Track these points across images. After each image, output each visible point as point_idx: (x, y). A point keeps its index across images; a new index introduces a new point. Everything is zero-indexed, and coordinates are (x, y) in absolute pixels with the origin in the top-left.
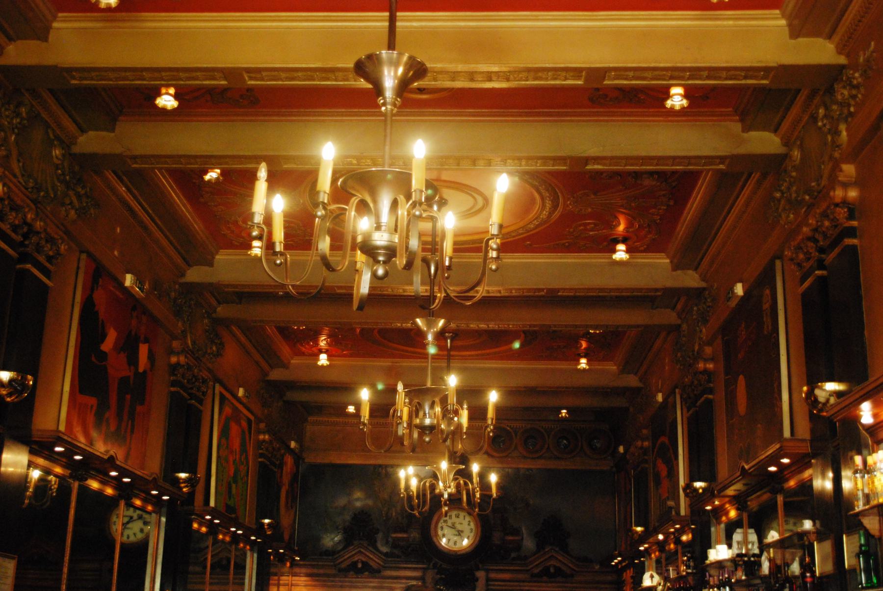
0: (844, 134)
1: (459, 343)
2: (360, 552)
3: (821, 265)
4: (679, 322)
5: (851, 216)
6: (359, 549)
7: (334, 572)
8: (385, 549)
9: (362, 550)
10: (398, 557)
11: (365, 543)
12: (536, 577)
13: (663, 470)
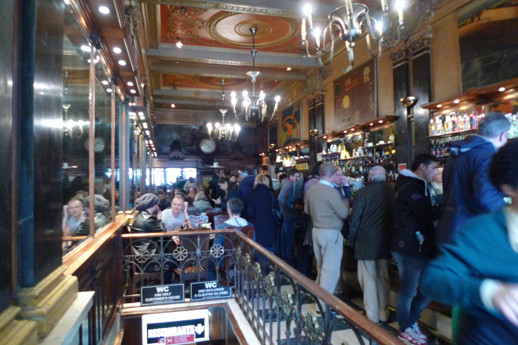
0: (433, 15)
1: (226, 84)
2: (177, 153)
3: (406, 59)
4: (306, 79)
5: (429, 43)
6: (176, 152)
7: (168, 160)
8: (184, 152)
9: (177, 153)
10: (189, 154)
11: (178, 150)
12: (232, 160)
13: (290, 127)
